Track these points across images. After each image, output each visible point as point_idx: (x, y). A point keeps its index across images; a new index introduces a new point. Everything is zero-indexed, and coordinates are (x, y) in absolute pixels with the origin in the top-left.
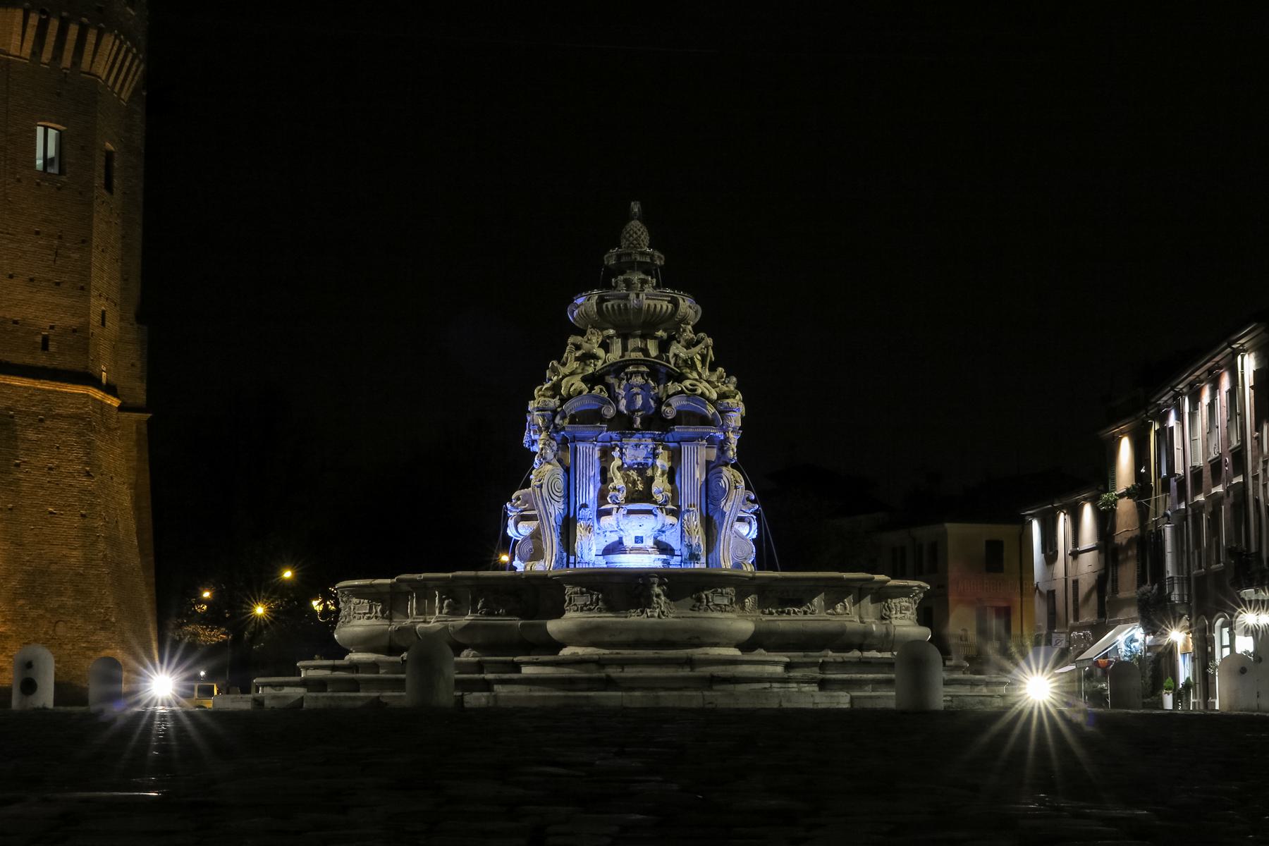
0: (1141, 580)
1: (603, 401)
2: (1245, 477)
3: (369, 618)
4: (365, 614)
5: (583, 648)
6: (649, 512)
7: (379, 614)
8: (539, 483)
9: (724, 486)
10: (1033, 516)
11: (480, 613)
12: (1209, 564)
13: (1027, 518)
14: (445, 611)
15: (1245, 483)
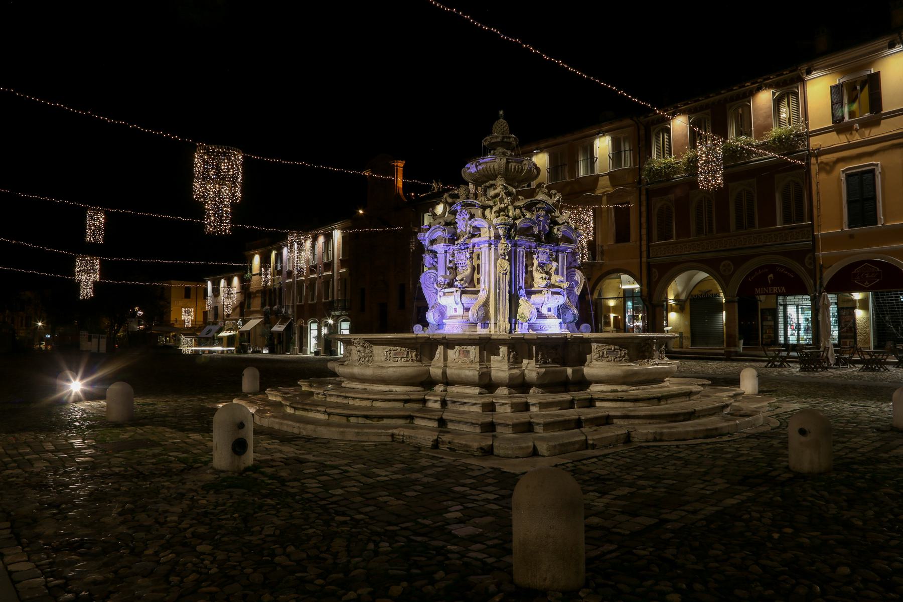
0: (263, 305)
1: (534, 223)
2: (333, 272)
3: (406, 361)
4: (402, 358)
5: (613, 386)
6: (558, 293)
7: (414, 358)
8: (505, 272)
9: (577, 280)
10: (209, 280)
11: (540, 362)
12: (306, 300)
13: (207, 280)
14: (511, 360)
15: (333, 275)
